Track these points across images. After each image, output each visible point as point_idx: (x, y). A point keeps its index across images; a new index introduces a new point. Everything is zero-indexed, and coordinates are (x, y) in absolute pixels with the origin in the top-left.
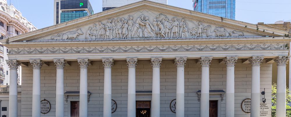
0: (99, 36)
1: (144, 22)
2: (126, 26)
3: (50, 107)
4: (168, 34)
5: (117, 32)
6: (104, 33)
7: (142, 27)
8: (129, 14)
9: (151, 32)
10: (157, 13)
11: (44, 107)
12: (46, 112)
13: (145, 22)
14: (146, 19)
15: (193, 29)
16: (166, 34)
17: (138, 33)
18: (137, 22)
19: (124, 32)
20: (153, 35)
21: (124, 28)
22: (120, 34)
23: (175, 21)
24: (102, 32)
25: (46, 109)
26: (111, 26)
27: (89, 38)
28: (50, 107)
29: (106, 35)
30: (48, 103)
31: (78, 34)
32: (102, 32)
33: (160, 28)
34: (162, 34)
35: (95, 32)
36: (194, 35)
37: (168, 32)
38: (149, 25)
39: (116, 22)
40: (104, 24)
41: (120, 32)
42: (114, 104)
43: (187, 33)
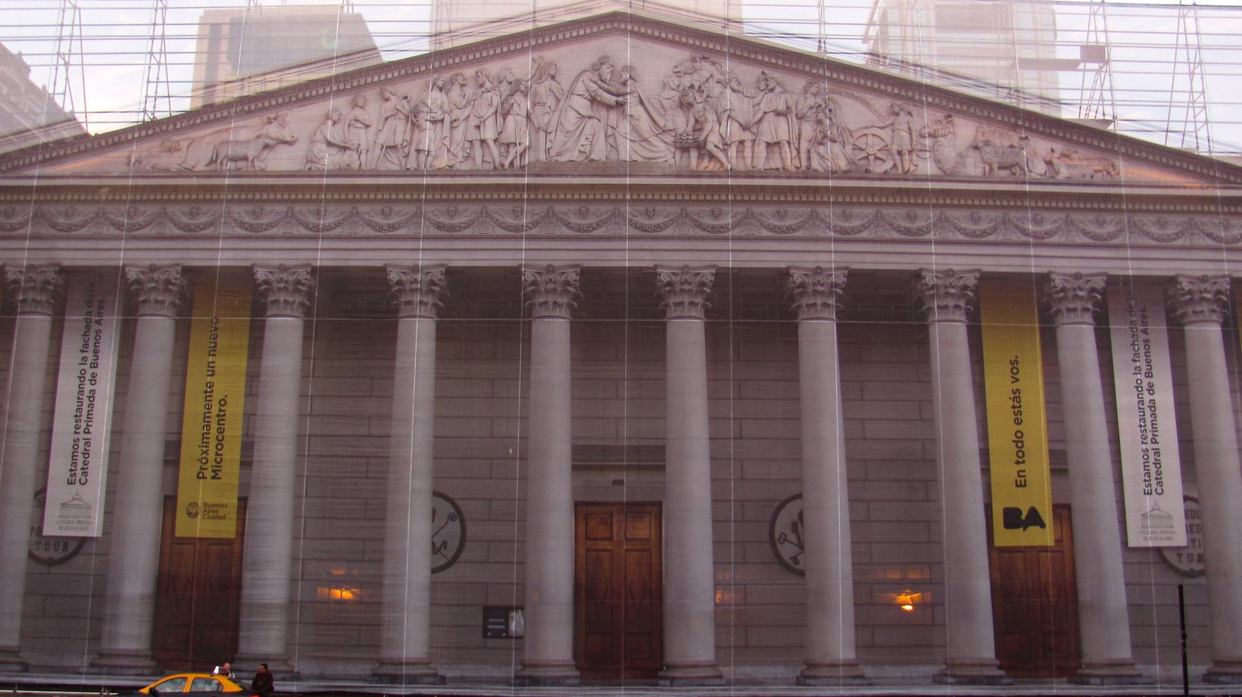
0: (378, 151)
1: (613, 89)
2: (523, 104)
4: (740, 152)
6: (407, 137)
7: (603, 113)
9: (653, 140)
13: (622, 90)
15: (866, 131)
16: (733, 151)
17: (582, 141)
18: (580, 88)
19: (509, 136)
20: (663, 152)
21: (510, 118)
22: (491, 143)
23: (772, 90)
24: (398, 131)
26: (446, 107)
27: (330, 159)
29: (413, 147)
31: (271, 142)
32: (398, 131)
33: (697, 121)
34: (710, 147)
35: (361, 137)
36: (872, 158)
37: (742, 142)
38: (642, 102)
39: (469, 91)
40: (406, 98)
41: (489, 133)
42: (451, 518)
43: (837, 148)
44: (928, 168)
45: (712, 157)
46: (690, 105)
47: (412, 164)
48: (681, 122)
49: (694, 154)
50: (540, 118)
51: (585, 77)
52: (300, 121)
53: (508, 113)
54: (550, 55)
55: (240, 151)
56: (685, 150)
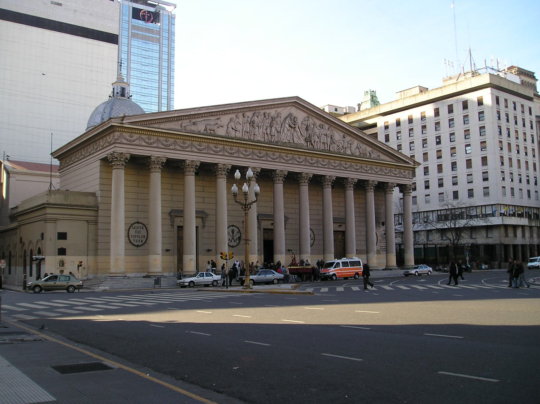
3: (147, 234)
8: (276, 109)
10: (305, 115)
11: (137, 234)
12: (140, 244)
14: (295, 119)
18: (287, 122)
20: (302, 142)
21: (273, 128)
24: (248, 127)
25: (141, 239)
27: (233, 134)
28: (147, 234)
30: (144, 227)
35: (239, 128)
41: (269, 132)
44: (349, 152)
45: (312, 144)
48: (305, 134)
50: (279, 129)
51: (289, 118)
52: (225, 119)
54: (279, 110)
55: (213, 128)
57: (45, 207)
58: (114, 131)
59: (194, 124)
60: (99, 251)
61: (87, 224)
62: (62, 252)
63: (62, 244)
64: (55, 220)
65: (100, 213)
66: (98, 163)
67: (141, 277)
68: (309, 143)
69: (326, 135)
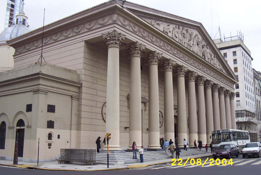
5: (188, 43)
45: (205, 58)
46: (203, 48)
47: (183, 44)
49: (204, 56)
53: (191, 40)
56: (203, 56)
57: (38, 78)
58: (114, 13)
59: (158, 24)
60: (82, 126)
61: (71, 99)
62: (51, 124)
63: (51, 117)
64: (46, 92)
65: (84, 90)
66: (83, 44)
67: (122, 151)
68: (204, 56)
69: (210, 54)
